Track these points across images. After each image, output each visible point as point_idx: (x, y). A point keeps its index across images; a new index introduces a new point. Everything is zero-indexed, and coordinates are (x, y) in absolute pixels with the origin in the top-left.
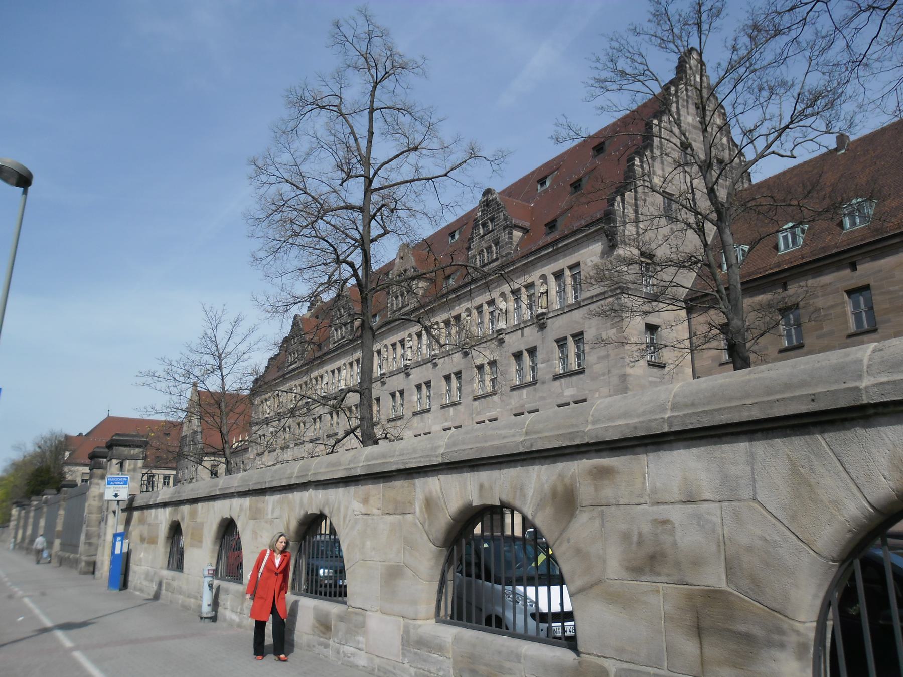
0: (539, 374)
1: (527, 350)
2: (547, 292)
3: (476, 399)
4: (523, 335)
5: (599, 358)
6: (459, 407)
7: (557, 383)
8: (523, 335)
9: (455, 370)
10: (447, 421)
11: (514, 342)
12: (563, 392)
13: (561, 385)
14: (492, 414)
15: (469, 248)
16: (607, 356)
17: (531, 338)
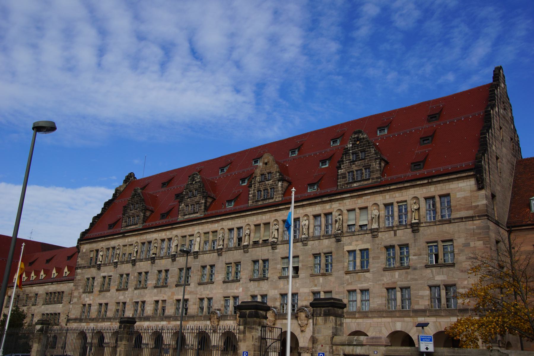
0: (411, 262)
1: (399, 245)
2: (418, 209)
3: (347, 273)
4: (395, 235)
6: (330, 278)
7: (428, 271)
8: (395, 235)
9: (325, 251)
10: (316, 286)
11: (386, 238)
12: (434, 277)
13: (432, 272)
14: (365, 285)
15: (339, 168)
17: (403, 238)
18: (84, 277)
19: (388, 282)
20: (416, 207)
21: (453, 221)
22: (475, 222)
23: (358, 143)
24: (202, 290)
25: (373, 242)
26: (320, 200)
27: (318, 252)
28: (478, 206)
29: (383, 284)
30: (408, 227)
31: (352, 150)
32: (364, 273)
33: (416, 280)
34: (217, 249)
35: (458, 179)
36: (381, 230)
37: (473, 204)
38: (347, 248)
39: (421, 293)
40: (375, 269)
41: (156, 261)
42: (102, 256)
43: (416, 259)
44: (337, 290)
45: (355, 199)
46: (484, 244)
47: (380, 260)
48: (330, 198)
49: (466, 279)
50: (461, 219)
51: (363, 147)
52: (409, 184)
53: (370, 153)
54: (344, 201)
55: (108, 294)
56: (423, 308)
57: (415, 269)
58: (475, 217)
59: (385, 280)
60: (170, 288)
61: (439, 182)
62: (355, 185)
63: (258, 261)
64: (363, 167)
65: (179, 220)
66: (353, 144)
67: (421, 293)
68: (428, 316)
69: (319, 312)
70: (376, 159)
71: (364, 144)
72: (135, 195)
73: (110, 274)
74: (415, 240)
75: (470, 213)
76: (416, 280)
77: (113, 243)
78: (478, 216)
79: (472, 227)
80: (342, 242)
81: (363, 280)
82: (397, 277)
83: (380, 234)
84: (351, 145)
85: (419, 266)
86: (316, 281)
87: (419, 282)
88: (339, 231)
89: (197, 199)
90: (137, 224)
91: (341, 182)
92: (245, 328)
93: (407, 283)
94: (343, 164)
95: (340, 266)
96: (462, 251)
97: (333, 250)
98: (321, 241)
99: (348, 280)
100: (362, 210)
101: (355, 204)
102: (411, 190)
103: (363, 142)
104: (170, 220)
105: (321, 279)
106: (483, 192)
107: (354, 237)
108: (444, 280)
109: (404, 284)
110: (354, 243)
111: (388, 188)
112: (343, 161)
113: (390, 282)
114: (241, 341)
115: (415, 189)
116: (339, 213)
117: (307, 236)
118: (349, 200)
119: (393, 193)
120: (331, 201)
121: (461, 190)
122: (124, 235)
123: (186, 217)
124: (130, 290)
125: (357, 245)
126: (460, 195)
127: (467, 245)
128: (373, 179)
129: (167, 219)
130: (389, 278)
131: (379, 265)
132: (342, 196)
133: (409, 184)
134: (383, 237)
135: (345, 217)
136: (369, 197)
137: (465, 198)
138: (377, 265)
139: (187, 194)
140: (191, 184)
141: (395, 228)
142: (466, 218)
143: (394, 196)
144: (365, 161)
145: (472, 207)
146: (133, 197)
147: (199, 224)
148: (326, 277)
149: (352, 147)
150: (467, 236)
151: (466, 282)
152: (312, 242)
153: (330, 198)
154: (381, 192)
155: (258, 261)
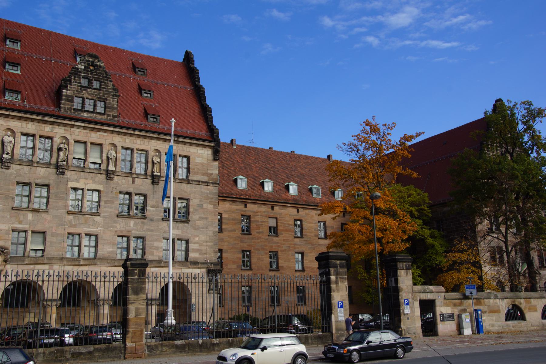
3: (69, 213)
4: (133, 182)
5: (200, 218)
6: (44, 215)
8: (133, 182)
10: (20, 222)
11: (123, 183)
16: (207, 218)
19: (121, 229)
20: (158, 160)
21: (191, 182)
22: (209, 187)
23: (91, 68)
25: (107, 184)
26: (40, 118)
27: (27, 181)
28: (212, 174)
29: (116, 231)
30: (149, 177)
31: (84, 73)
32: (93, 217)
33: (152, 231)
35: (199, 145)
36: (117, 174)
37: (209, 172)
38: (71, 184)
39: (156, 244)
40: (107, 214)
43: (153, 211)
44: (54, 231)
45: (88, 131)
46: (214, 208)
47: (113, 206)
48: (56, 120)
49: (198, 236)
50: (198, 182)
51: (100, 76)
52: (155, 136)
53: (108, 86)
54: (72, 129)
56: (157, 259)
57: (152, 220)
58: (210, 183)
59: (118, 227)
61: (182, 143)
62: (85, 114)
64: (97, 98)
66: (85, 67)
67: (156, 244)
68: (162, 267)
69: (401, 266)
70: (113, 95)
71: (101, 73)
74: (154, 192)
75: (205, 179)
76: (152, 231)
78: (212, 183)
79: (206, 191)
80: (65, 176)
81: (91, 223)
82: (132, 225)
83: (115, 177)
84: (83, 67)
85: (155, 218)
86: (22, 218)
87: (155, 233)
88: (65, 163)
91: (64, 104)
92: (337, 278)
93: (142, 233)
94: (70, 84)
95: (61, 203)
96: (196, 210)
97: (51, 183)
98: (33, 168)
99: (70, 221)
100: (93, 146)
101: (87, 136)
102: (153, 141)
103: (99, 70)
105: (30, 216)
106: (217, 163)
107: (82, 174)
108: (179, 235)
109: (141, 233)
110: (82, 180)
111: (132, 132)
112: (70, 81)
113: (124, 229)
114: (334, 291)
115: (158, 142)
116: (64, 141)
117: (10, 157)
118: (79, 130)
119: (134, 138)
120: (53, 123)
121: (199, 156)
125: (86, 184)
126: (198, 160)
127: (201, 206)
128: (108, 115)
130: (122, 225)
131: (113, 210)
132: (73, 123)
133: (155, 136)
134: (120, 182)
135: (71, 148)
136: (106, 134)
137: (202, 164)
138: (110, 210)
141: (134, 176)
142: (202, 182)
143: (135, 142)
144: (100, 93)
145: (207, 173)
148: (38, 214)
149: (84, 70)
150: (201, 199)
151: (197, 239)
152: (19, 167)
153: (56, 120)
154: (122, 133)
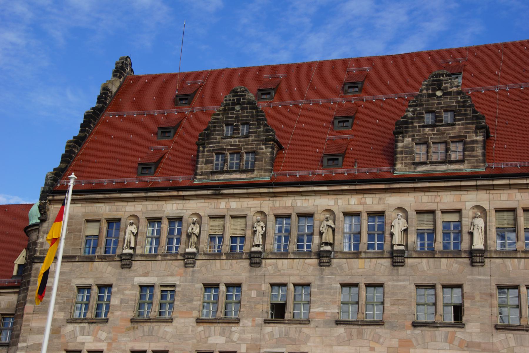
18: (69, 282)
24: (512, 344)
34: (251, 253)
41: (334, 261)
42: (136, 236)
55: (168, 329)
60: (393, 327)
63: (216, 286)
65: (397, 173)
72: (234, 104)
73: (170, 280)
77: (172, 208)
89: (458, 130)
90: (252, 171)
104: (150, 180)
122: (217, 190)
123: (421, 168)
124: (247, 322)
129: (375, 168)
139: (420, 117)
140: (429, 95)
146: (230, 107)
147: (477, 188)
155: (216, 286)
